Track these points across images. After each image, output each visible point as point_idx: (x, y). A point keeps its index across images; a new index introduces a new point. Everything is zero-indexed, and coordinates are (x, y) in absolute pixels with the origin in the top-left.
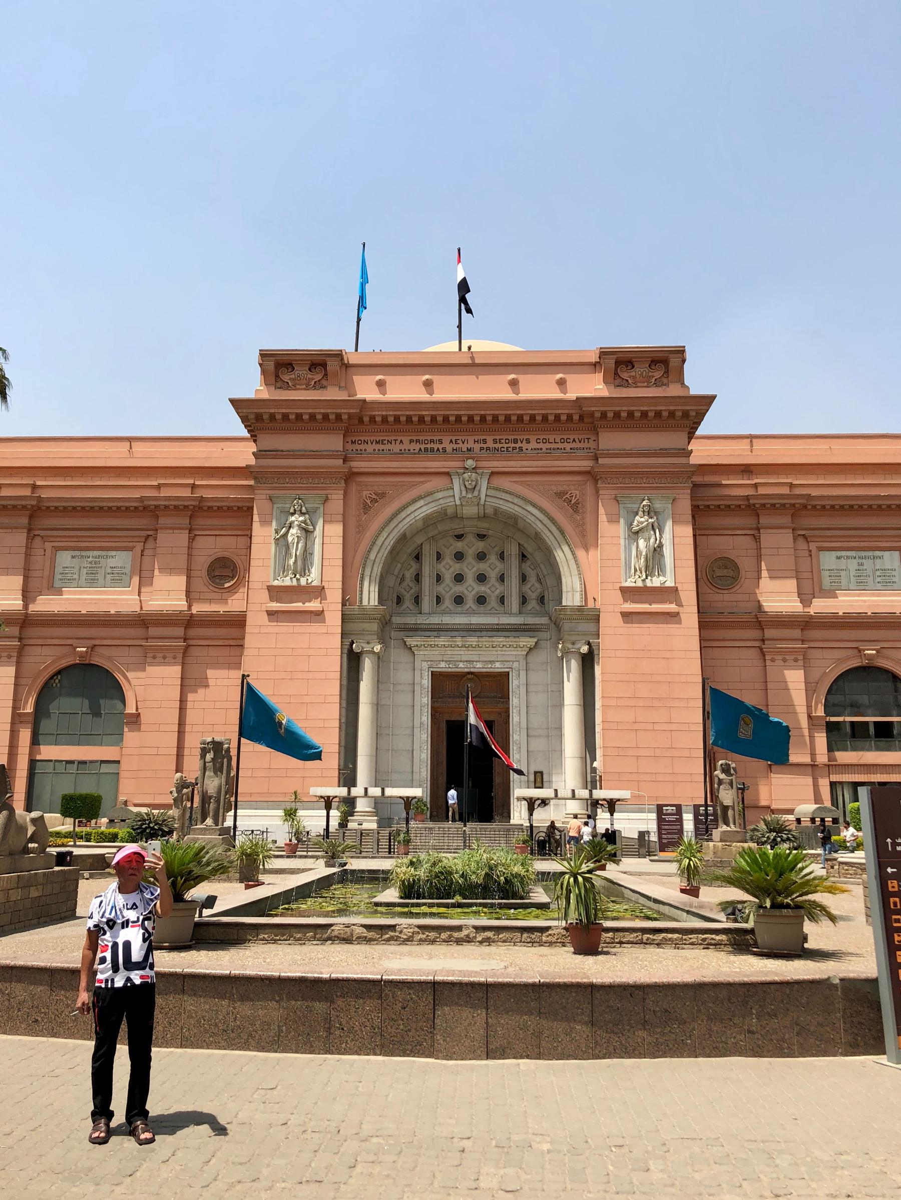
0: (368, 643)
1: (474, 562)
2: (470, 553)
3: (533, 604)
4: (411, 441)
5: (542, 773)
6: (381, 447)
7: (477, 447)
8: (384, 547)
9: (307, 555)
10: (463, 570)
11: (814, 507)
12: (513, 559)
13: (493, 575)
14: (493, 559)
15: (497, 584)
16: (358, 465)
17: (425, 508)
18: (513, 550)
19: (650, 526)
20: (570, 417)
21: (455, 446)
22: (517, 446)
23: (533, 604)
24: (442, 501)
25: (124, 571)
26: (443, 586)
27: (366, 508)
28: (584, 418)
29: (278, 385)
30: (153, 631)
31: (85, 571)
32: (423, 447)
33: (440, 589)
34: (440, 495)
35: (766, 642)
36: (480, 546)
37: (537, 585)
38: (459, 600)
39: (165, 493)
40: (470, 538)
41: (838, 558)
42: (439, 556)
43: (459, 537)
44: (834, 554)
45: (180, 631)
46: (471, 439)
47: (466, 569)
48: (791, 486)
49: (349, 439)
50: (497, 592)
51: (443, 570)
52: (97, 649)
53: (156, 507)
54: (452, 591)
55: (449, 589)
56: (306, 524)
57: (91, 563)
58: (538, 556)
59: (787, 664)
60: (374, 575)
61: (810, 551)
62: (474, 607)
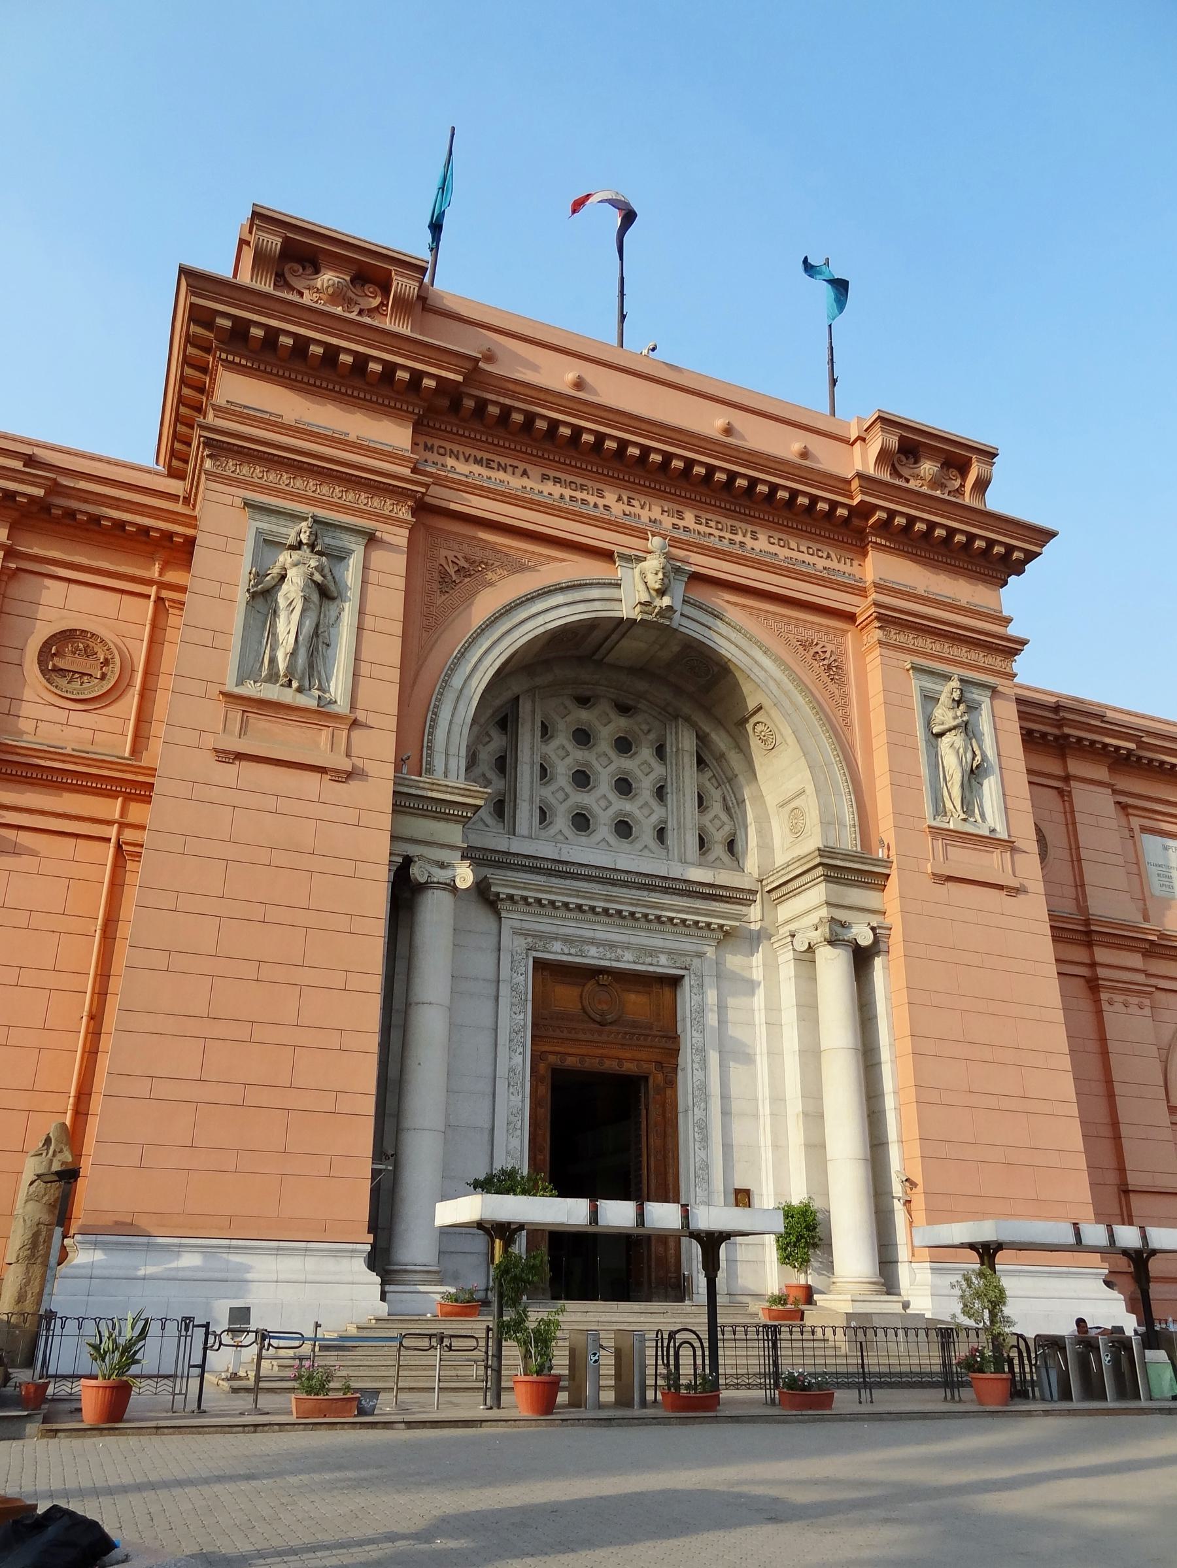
0: (442, 866)
1: (612, 754)
2: (606, 733)
3: (719, 850)
4: (545, 477)
6: (485, 472)
7: (667, 522)
8: (482, 668)
9: (316, 643)
10: (588, 764)
12: (686, 759)
13: (645, 787)
15: (654, 803)
16: (440, 496)
17: (564, 611)
18: (688, 742)
21: (628, 509)
22: (738, 538)
24: (597, 605)
26: (553, 787)
27: (445, 581)
32: (567, 492)
33: (546, 792)
34: (595, 593)
37: (724, 817)
38: (582, 822)
40: (605, 706)
43: (583, 701)
49: (422, 440)
50: (654, 818)
51: (553, 757)
54: (570, 802)
58: (735, 760)
59: (1130, 1010)
60: (458, 720)
61: (1131, 830)
62: (612, 839)
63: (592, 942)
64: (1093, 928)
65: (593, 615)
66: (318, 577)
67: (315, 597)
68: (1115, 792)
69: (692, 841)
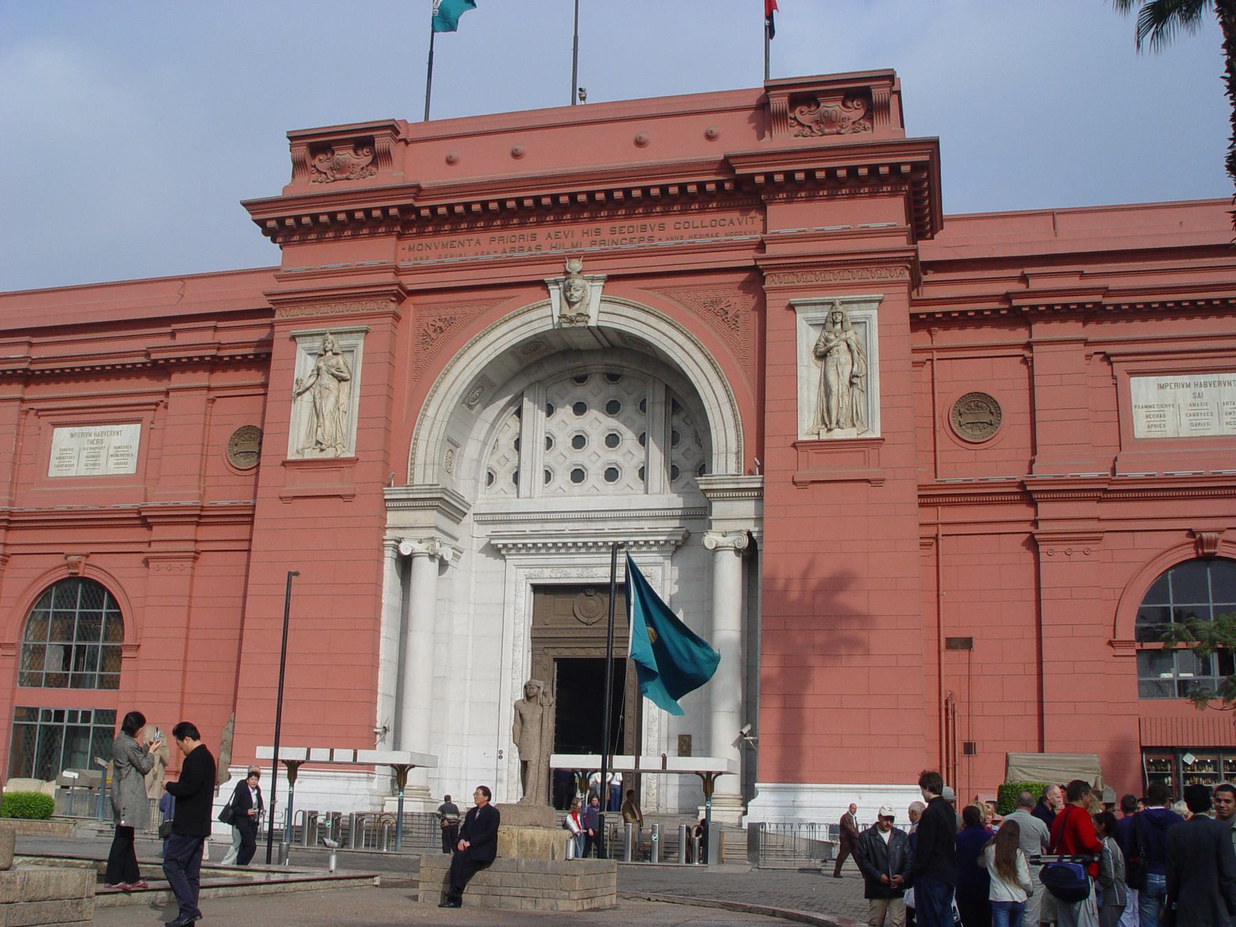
0: (420, 542)
4: (493, 239)
5: (689, 736)
11: (1117, 306)
14: (629, 409)
19: (843, 346)
20: (719, 184)
22: (646, 235)
23: (685, 477)
24: (535, 325)
25: (130, 451)
28: (740, 188)
29: (314, 177)
30: (158, 532)
31: (85, 453)
32: (508, 246)
33: (551, 458)
35: (1040, 524)
36: (612, 391)
37: (695, 448)
39: (181, 339)
40: (595, 383)
41: (1161, 387)
42: (550, 411)
43: (581, 380)
44: (1152, 379)
45: (188, 532)
46: (577, 229)
47: (589, 430)
48: (1082, 275)
52: (95, 560)
53: (167, 360)
55: (565, 458)
56: (338, 369)
57: (92, 442)
61: (1114, 377)
63: (574, 566)
64: (1028, 488)
65: (532, 333)
66: (333, 371)
67: (333, 383)
68: (1086, 342)
69: (658, 472)
